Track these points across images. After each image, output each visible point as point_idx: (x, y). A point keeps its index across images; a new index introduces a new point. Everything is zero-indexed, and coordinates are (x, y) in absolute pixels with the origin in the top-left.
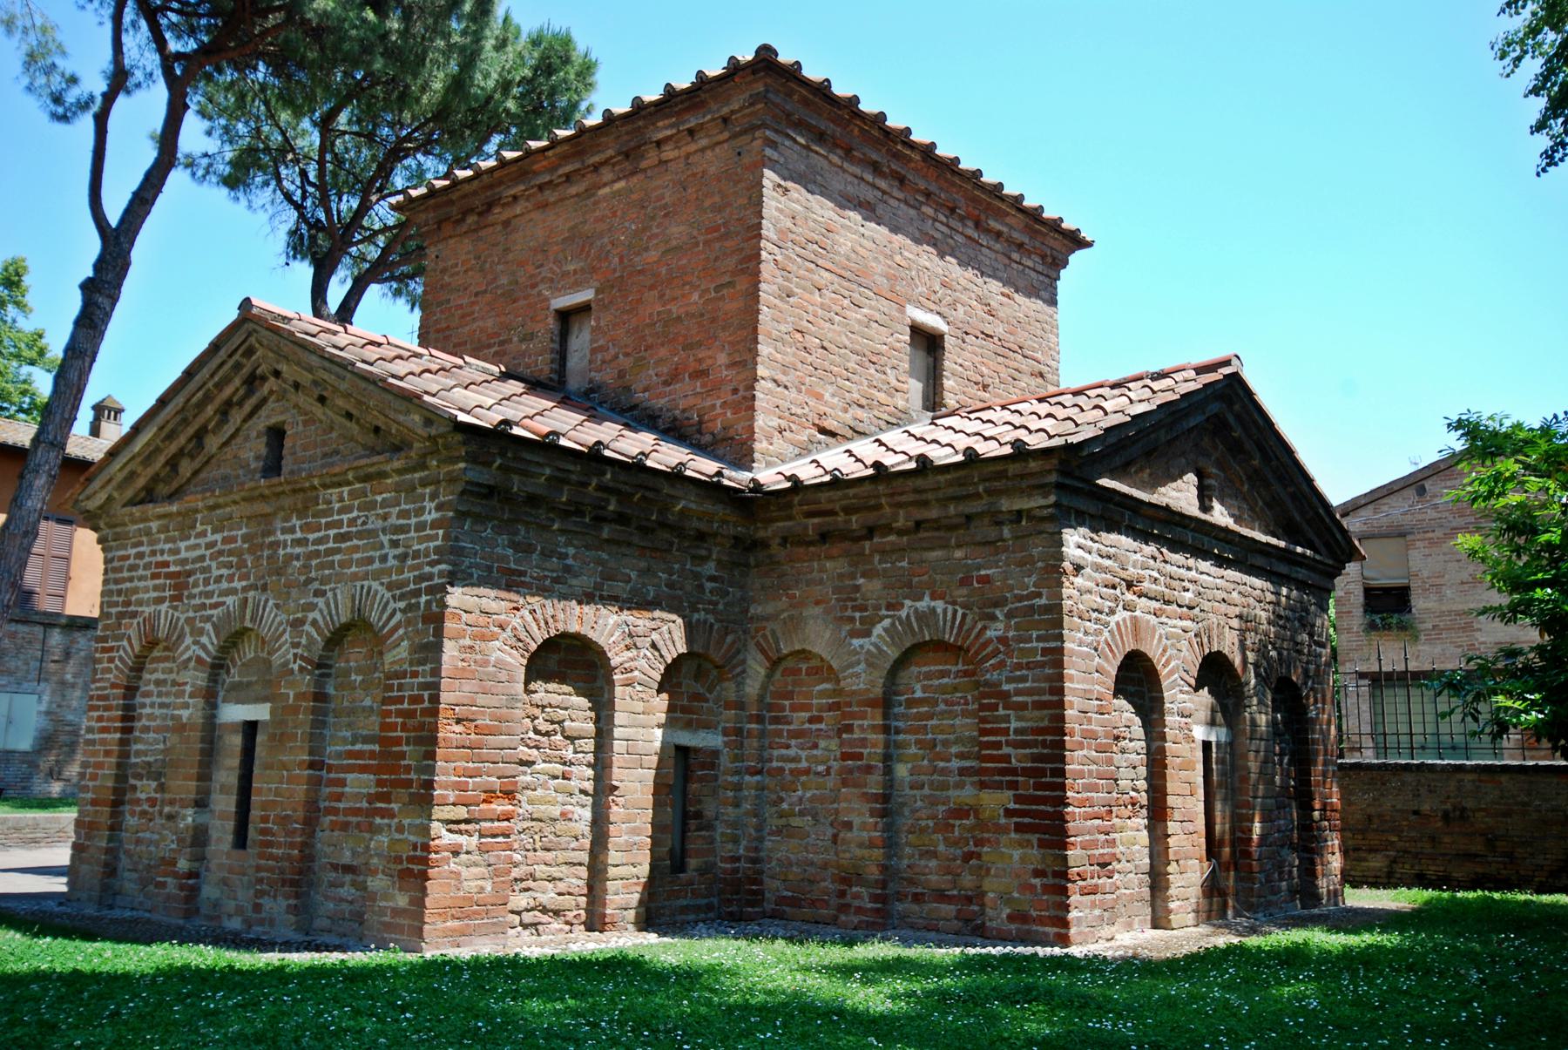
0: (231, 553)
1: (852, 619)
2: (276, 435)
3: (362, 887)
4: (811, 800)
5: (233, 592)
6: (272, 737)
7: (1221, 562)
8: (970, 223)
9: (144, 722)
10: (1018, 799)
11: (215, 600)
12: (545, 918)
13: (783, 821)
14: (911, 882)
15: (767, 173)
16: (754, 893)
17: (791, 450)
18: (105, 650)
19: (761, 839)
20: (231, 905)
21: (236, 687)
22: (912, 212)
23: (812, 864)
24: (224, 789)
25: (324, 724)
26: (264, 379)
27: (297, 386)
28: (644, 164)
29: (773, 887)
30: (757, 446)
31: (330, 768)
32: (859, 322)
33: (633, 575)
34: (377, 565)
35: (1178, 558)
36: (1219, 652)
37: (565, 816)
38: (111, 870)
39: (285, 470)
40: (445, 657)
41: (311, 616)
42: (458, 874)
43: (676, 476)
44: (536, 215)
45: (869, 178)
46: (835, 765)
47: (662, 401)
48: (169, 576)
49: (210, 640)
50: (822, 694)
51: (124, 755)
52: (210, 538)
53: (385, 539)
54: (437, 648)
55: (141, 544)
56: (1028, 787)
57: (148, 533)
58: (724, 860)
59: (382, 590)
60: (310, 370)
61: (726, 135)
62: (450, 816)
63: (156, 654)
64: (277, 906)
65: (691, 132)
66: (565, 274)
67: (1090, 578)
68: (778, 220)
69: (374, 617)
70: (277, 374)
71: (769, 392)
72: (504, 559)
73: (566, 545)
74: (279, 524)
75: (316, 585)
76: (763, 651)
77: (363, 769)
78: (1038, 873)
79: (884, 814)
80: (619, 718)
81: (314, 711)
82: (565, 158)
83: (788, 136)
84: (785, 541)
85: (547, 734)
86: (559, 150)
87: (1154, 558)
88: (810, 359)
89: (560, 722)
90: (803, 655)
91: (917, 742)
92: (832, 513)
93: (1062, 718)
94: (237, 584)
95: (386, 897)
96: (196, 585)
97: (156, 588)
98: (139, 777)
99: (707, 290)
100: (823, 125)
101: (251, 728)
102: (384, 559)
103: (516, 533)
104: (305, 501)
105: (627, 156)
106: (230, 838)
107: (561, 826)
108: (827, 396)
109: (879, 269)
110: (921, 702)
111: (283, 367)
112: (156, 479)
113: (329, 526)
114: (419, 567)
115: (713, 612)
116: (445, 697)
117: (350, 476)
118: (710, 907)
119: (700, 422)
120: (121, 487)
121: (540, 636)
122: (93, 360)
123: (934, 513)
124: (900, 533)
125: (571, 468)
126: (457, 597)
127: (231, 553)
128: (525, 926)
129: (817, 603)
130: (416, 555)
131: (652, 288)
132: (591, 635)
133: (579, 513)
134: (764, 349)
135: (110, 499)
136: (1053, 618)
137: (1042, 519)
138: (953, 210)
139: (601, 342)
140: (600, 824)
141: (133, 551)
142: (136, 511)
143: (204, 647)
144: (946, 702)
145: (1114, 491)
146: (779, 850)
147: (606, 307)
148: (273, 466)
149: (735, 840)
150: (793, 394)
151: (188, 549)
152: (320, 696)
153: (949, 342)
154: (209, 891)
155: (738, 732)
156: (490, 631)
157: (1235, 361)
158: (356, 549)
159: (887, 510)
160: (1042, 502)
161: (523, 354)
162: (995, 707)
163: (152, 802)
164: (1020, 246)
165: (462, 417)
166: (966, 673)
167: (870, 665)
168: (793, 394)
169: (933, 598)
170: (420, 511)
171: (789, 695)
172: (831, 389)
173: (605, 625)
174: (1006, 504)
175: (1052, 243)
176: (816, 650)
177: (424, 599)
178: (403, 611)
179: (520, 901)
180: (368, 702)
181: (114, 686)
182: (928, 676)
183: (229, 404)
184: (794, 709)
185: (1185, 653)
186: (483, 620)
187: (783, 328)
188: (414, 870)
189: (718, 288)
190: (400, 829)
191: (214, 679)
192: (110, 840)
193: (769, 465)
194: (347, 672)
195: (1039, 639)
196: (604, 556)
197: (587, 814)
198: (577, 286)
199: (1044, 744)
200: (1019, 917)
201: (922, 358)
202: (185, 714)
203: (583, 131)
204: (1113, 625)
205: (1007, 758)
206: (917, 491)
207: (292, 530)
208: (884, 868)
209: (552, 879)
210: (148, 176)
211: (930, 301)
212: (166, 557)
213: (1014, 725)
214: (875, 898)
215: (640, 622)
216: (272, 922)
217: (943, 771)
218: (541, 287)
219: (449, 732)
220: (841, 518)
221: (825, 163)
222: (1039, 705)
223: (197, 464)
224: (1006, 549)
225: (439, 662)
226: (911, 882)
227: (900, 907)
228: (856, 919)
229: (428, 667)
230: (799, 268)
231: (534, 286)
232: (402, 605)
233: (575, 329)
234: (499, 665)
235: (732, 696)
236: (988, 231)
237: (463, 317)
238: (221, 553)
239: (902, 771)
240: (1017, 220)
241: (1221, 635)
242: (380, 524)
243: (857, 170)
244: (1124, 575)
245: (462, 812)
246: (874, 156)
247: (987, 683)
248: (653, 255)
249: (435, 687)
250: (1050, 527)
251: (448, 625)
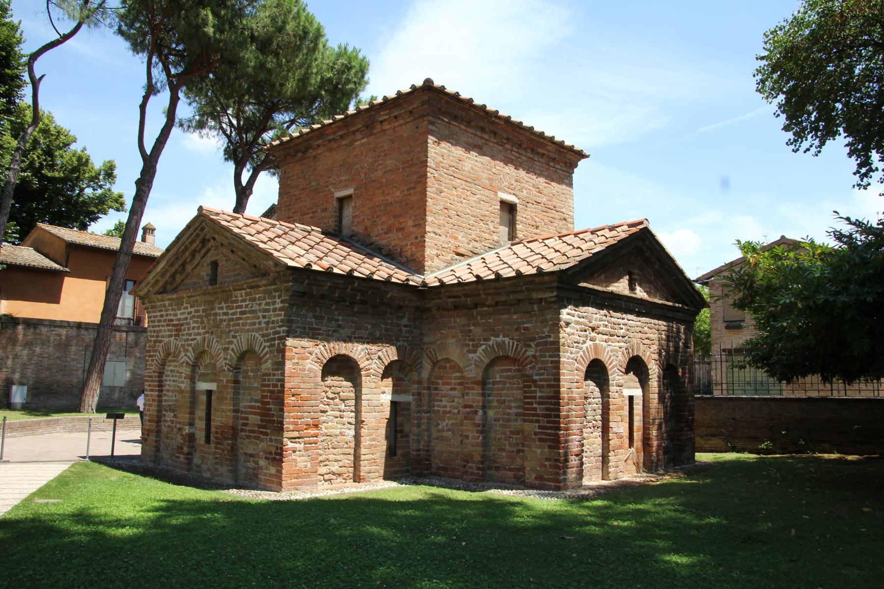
0: (198, 317)
1: (468, 345)
2: (215, 265)
3: (257, 463)
4: (452, 424)
5: (199, 334)
6: (218, 398)
7: (639, 314)
8: (529, 151)
9: (167, 388)
10: (540, 427)
11: (192, 337)
12: (334, 477)
13: (439, 434)
14: (495, 462)
15: (430, 137)
16: (427, 465)
17: (442, 264)
18: (150, 356)
19: (430, 441)
20: (204, 467)
21: (203, 375)
22: (501, 148)
23: (452, 452)
24: (200, 419)
25: (238, 393)
26: (209, 241)
27: (222, 245)
28: (375, 131)
29: (436, 462)
30: (426, 263)
31: (242, 412)
32: (475, 202)
33: (369, 327)
34: (257, 326)
35: (619, 315)
36: (638, 356)
37: (342, 434)
38: (158, 450)
39: (218, 281)
40: (286, 368)
41: (231, 346)
42: (296, 460)
43: (387, 282)
44: (327, 154)
45: (479, 134)
46: (461, 409)
47: (384, 242)
48: (174, 325)
50: (456, 378)
51: (160, 401)
52: (190, 310)
53: (260, 314)
54: (283, 364)
55: (161, 311)
56: (544, 421)
57: (164, 306)
58: (413, 450)
59: (260, 337)
60: (227, 238)
61: (411, 119)
62: (292, 436)
63: (170, 358)
64: (224, 470)
65: (396, 117)
66: (341, 181)
67: (573, 328)
68: (435, 158)
69: (257, 349)
70: (214, 239)
71: (432, 238)
72: (311, 323)
73: (339, 315)
74: (217, 305)
75: (232, 333)
76: (429, 358)
77: (255, 414)
78: (547, 460)
79: (482, 432)
80: (364, 391)
81: (234, 388)
82: (340, 128)
83: (440, 119)
84: (438, 309)
85: (332, 399)
86: (337, 124)
87: (606, 316)
88: (451, 221)
89: (338, 393)
90: (448, 360)
91: (498, 401)
92: (458, 297)
93: (559, 392)
94: (201, 331)
95: (267, 469)
96: (184, 330)
97: (169, 330)
98: (167, 411)
99: (403, 191)
101: (209, 393)
102: (260, 323)
103: (316, 311)
104: (227, 297)
105: (367, 127)
106: (204, 439)
107: (340, 438)
108: (460, 237)
109: (485, 176)
110: (499, 382)
111: (216, 236)
112: (166, 283)
113: (237, 307)
114: (274, 328)
115: (406, 341)
116: (287, 385)
117: (245, 286)
118: (408, 471)
119: (401, 252)
120: (152, 286)
121: (328, 356)
122: (142, 216)
123: (503, 299)
124: (489, 306)
125: (339, 282)
126: (290, 342)
127: (198, 317)
128: (326, 481)
129: (453, 337)
130: (273, 322)
131: (379, 188)
132: (351, 355)
133: (344, 300)
134: (429, 218)
135: (149, 291)
136: (554, 348)
137: (552, 302)
139: (357, 213)
140: (357, 437)
141: (159, 314)
142: (159, 296)
143: (189, 358)
144: (510, 383)
145: (585, 288)
146: (438, 447)
148: (213, 280)
149: (418, 442)
150: (443, 238)
151: (181, 314)
152: (236, 382)
153: (519, 207)
154: (197, 460)
155: (419, 394)
156: (305, 357)
157: (645, 222)
158: (248, 318)
159: (483, 296)
160: (551, 295)
161: (323, 218)
162: (530, 387)
163: (172, 421)
164: (554, 159)
165: (291, 263)
166: (519, 370)
167: (477, 366)
168: (443, 238)
169: (504, 337)
170: (274, 303)
171: (441, 378)
172: (462, 234)
173: (357, 351)
174: (535, 296)
175: (569, 157)
176: (453, 358)
177: (277, 342)
178: (269, 347)
179: (323, 470)
180: (256, 385)
181: (154, 372)
182: (502, 371)
183: (195, 251)
184: (444, 384)
185: (620, 357)
186: (302, 351)
187: (438, 207)
188: (277, 457)
189: (408, 190)
190: (271, 440)
191: (193, 371)
192: (157, 437)
193: (432, 272)
194: (247, 371)
195: (550, 356)
196: (356, 319)
197: (352, 432)
198: (346, 187)
199: (551, 404)
200: (540, 478)
201: (506, 216)
202: (183, 386)
203: (347, 116)
204: (584, 348)
205: (535, 409)
206: (495, 288)
207: (222, 308)
208: (483, 456)
209: (336, 461)
210: (163, 130)
211: (510, 189)
212: (172, 317)
213: (539, 394)
214: (478, 469)
215: (373, 348)
216: (222, 476)
217: (509, 414)
218: (330, 187)
219: (289, 400)
220: (463, 299)
221: (457, 129)
222: (549, 386)
223: (183, 277)
224: (536, 315)
225: (284, 370)
226: (495, 462)
227: (490, 472)
228: (470, 477)
229: (279, 372)
230: (446, 179)
231: (327, 186)
232: (268, 344)
233: (346, 206)
234: (310, 370)
235: (416, 378)
236: (538, 154)
237: (296, 200)
238: (194, 317)
239: (491, 413)
240: (551, 147)
241: (638, 348)
242: (258, 307)
243: (474, 131)
244: (591, 325)
245: (296, 434)
246: (481, 124)
247: (527, 376)
248: (380, 173)
249: (283, 381)
250: (555, 306)
251: (287, 354)
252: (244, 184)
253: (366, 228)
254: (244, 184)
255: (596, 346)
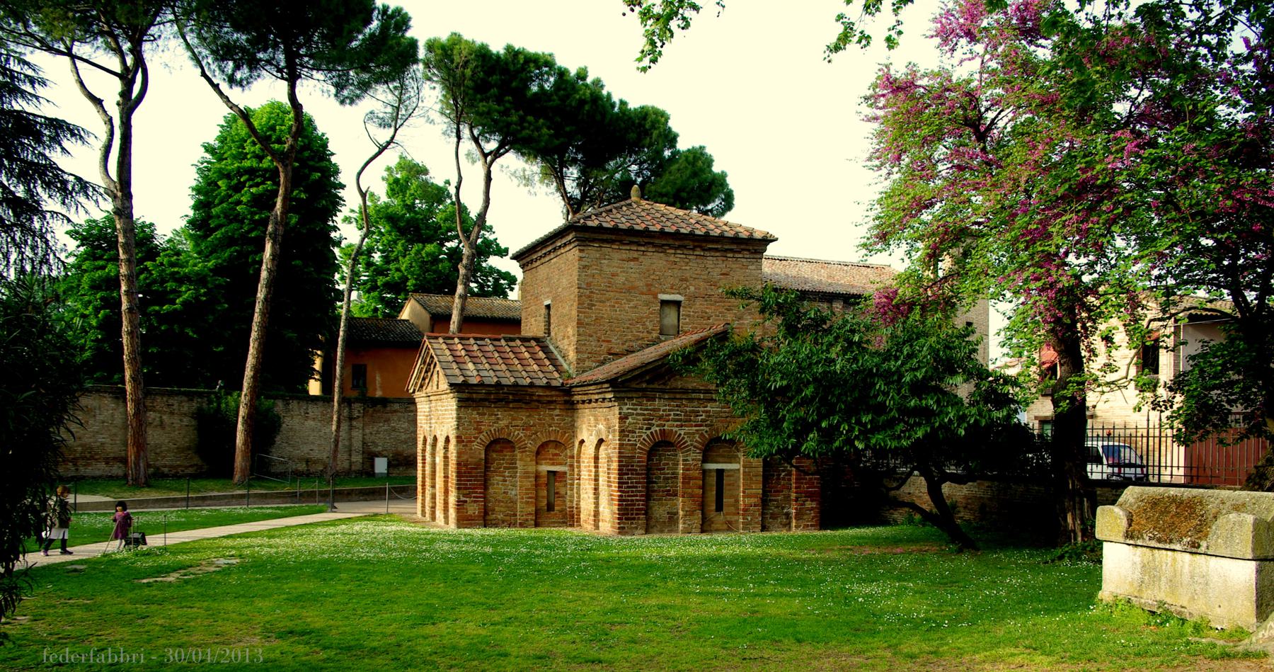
100: (605, 237)
133: (501, 400)
138: (685, 247)
255: (663, 432)
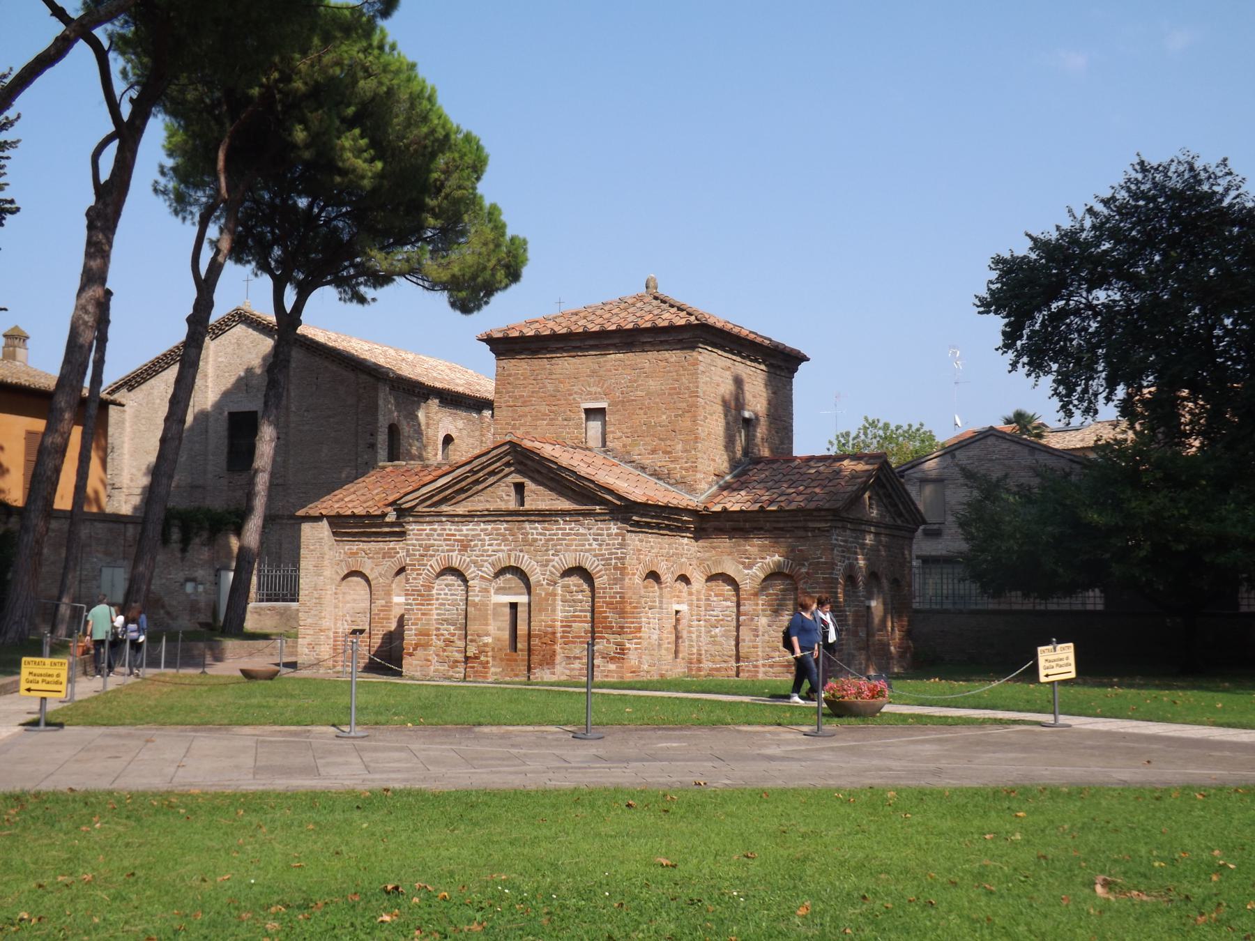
17: (706, 486)
49: (489, 570)
66: (590, 393)
69: (587, 566)
96: (476, 545)
101: (514, 606)
123: (781, 525)
147: (613, 413)
174: (811, 525)
184: (716, 595)
189: (676, 416)
198: (596, 399)
202: (477, 599)
207: (536, 528)
252: (288, 311)
253: (625, 446)
254: (288, 311)
